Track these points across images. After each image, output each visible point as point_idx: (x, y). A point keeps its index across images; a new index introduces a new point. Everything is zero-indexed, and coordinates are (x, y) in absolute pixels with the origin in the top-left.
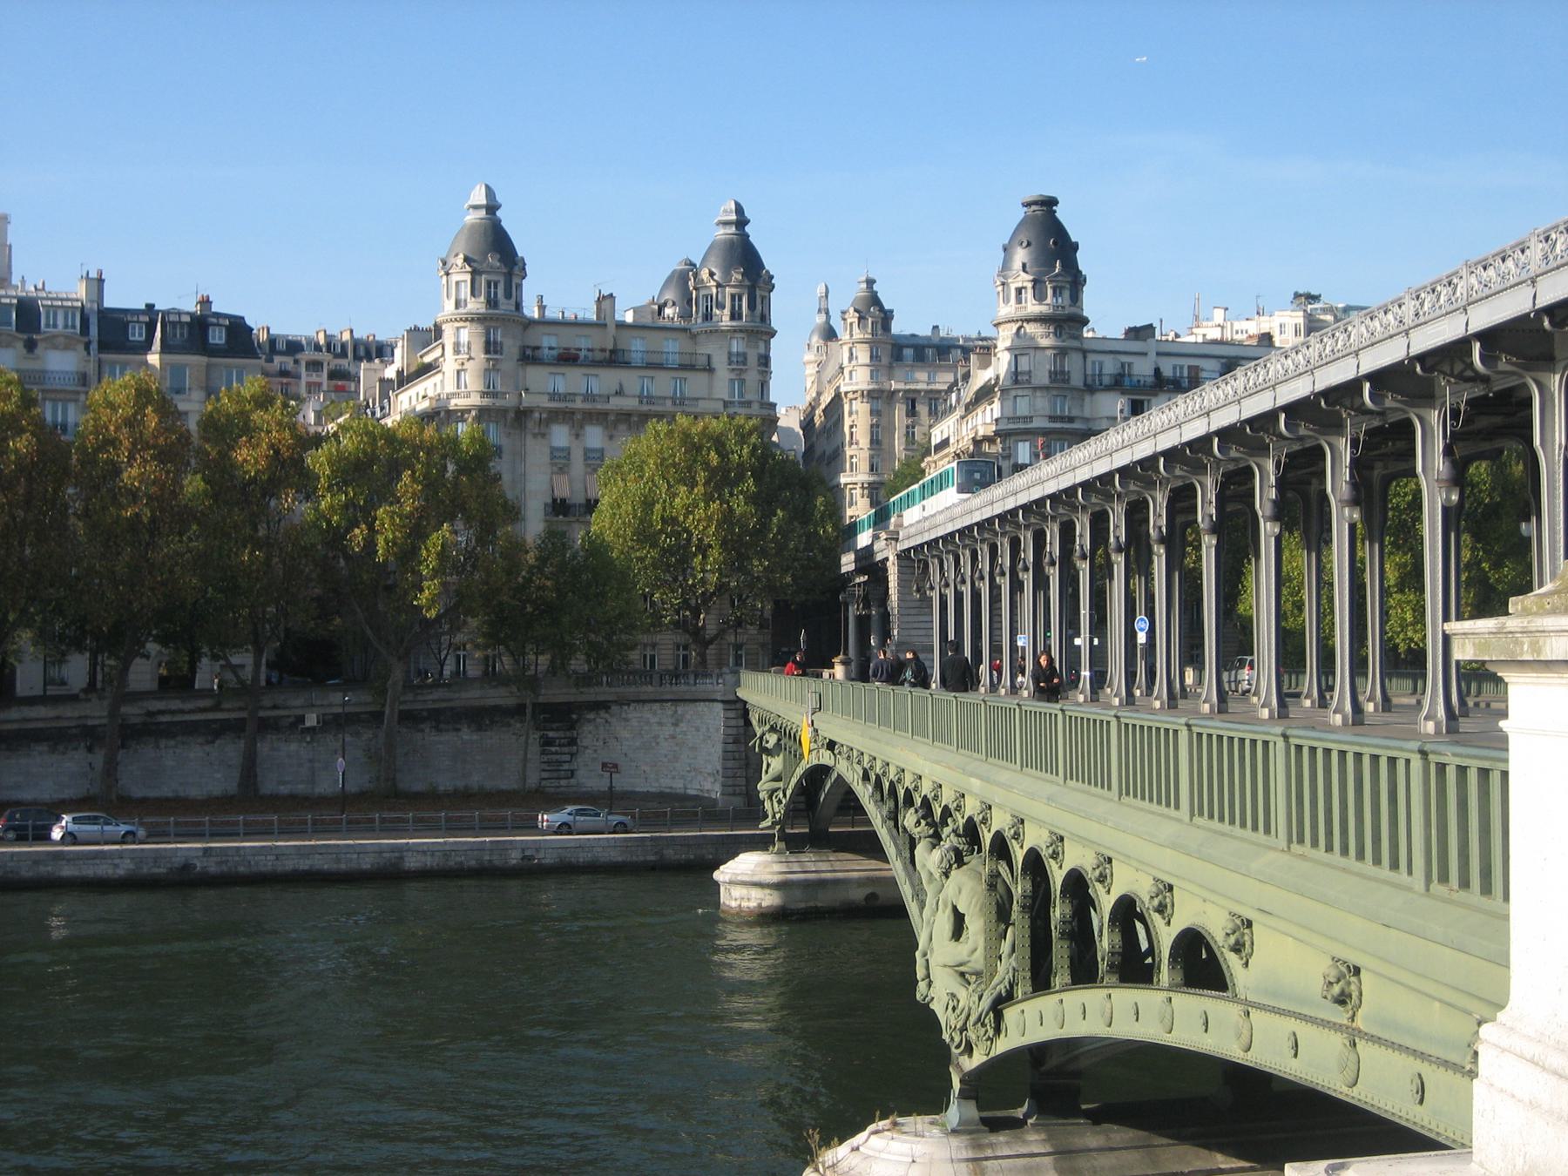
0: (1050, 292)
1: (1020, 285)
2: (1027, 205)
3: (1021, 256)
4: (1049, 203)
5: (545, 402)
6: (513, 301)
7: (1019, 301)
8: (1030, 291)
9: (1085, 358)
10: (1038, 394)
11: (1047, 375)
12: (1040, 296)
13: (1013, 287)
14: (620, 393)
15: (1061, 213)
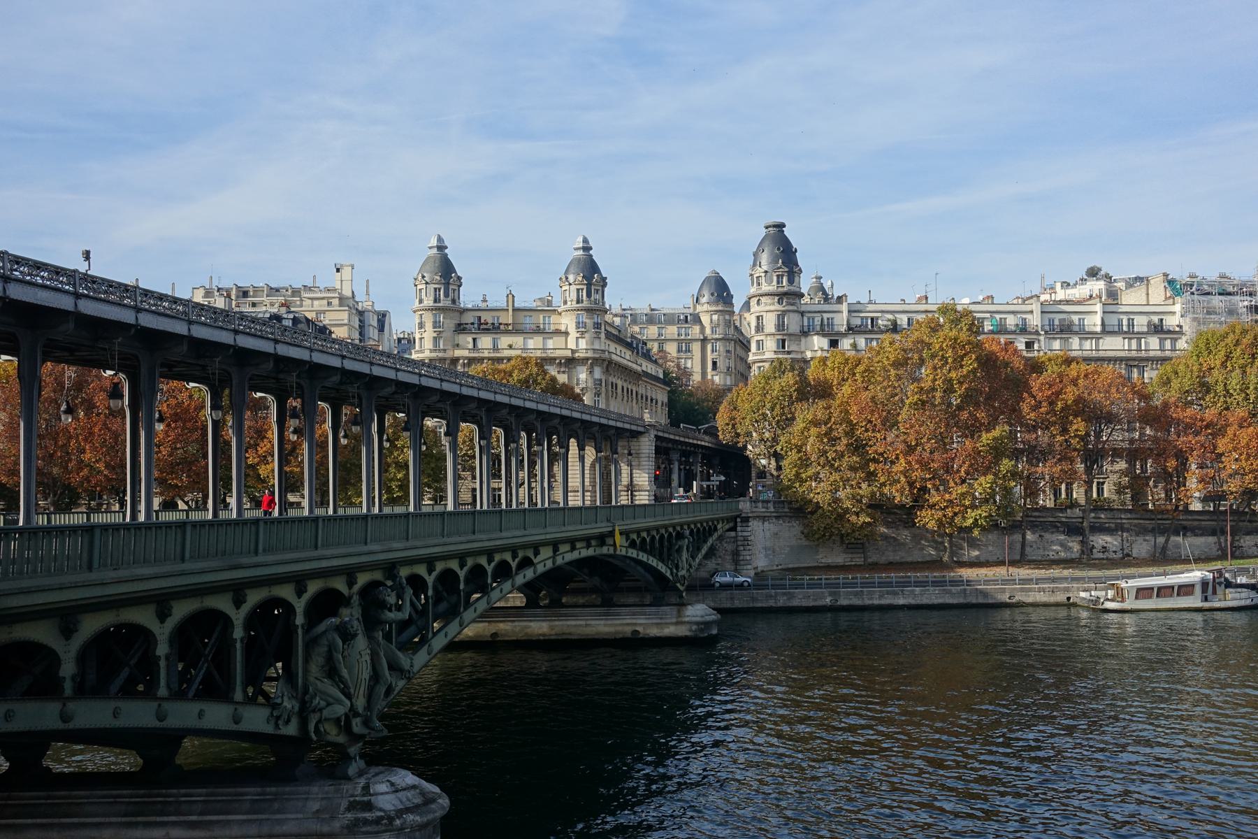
0: (775, 278)
1: (758, 275)
2: (767, 228)
3: (765, 258)
4: (780, 226)
5: (466, 353)
6: (450, 298)
7: (759, 284)
8: (763, 278)
9: (802, 316)
10: (769, 338)
11: (773, 327)
12: (770, 282)
13: (755, 276)
14: (510, 347)
15: (787, 231)
